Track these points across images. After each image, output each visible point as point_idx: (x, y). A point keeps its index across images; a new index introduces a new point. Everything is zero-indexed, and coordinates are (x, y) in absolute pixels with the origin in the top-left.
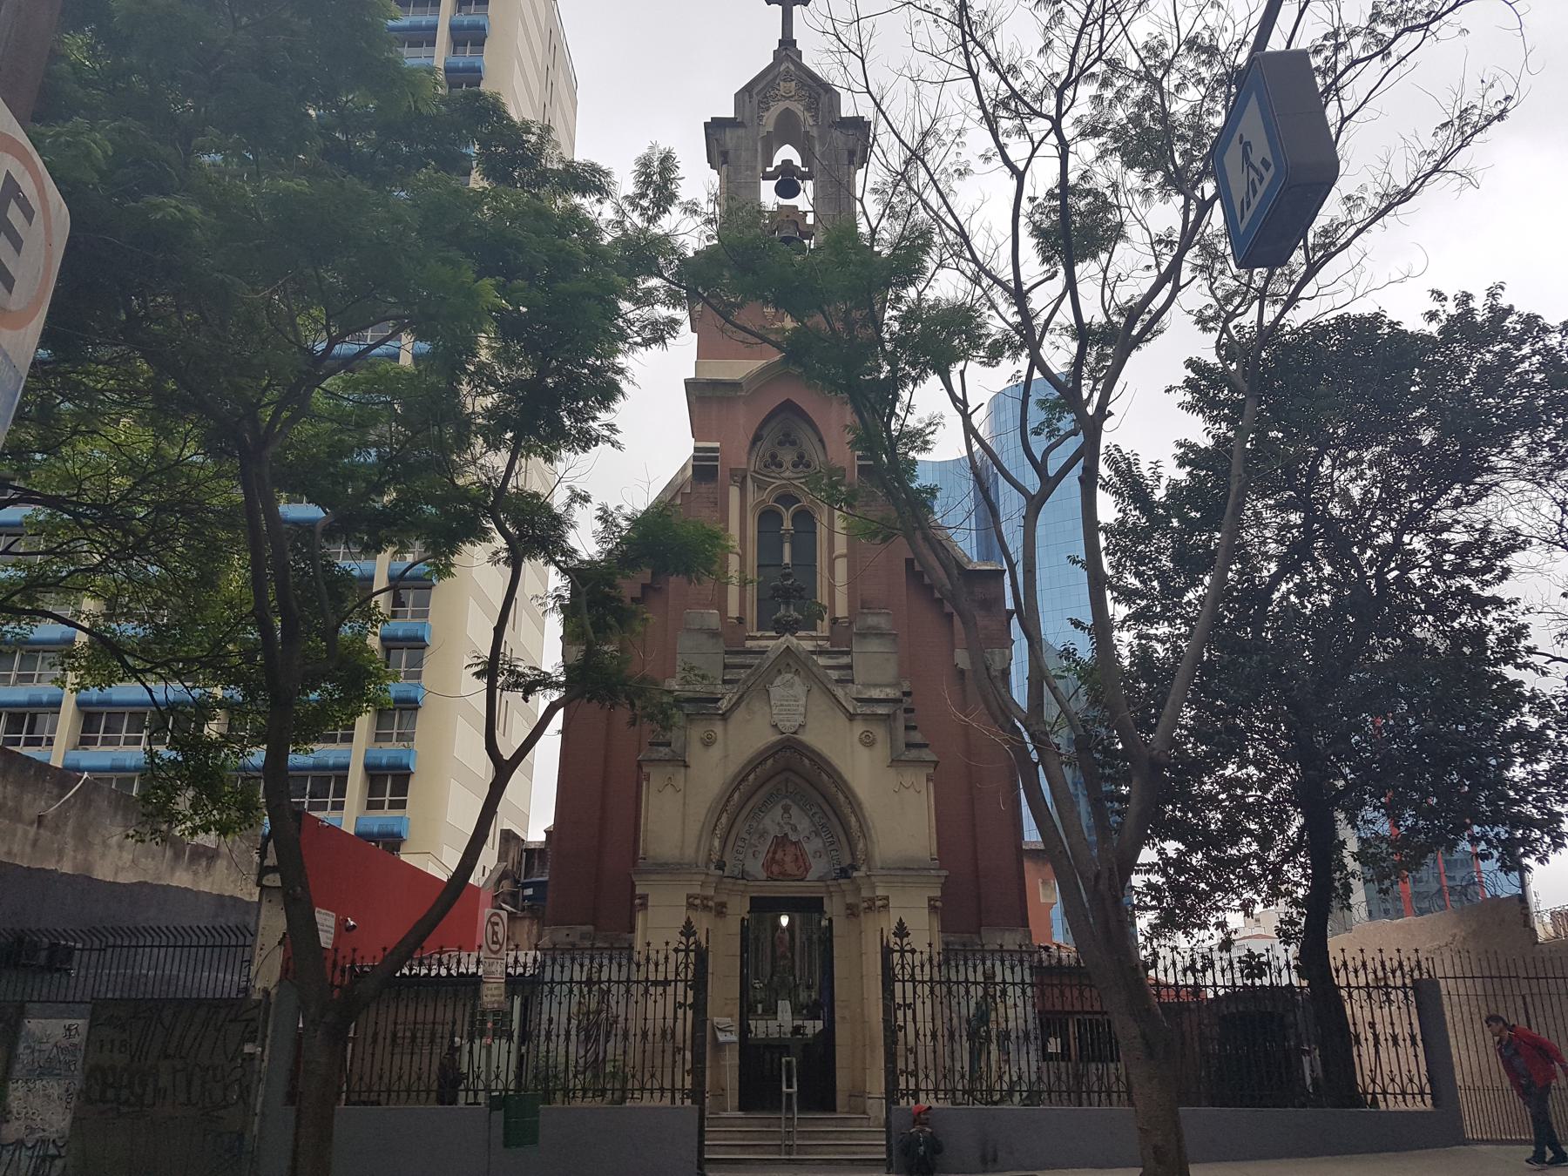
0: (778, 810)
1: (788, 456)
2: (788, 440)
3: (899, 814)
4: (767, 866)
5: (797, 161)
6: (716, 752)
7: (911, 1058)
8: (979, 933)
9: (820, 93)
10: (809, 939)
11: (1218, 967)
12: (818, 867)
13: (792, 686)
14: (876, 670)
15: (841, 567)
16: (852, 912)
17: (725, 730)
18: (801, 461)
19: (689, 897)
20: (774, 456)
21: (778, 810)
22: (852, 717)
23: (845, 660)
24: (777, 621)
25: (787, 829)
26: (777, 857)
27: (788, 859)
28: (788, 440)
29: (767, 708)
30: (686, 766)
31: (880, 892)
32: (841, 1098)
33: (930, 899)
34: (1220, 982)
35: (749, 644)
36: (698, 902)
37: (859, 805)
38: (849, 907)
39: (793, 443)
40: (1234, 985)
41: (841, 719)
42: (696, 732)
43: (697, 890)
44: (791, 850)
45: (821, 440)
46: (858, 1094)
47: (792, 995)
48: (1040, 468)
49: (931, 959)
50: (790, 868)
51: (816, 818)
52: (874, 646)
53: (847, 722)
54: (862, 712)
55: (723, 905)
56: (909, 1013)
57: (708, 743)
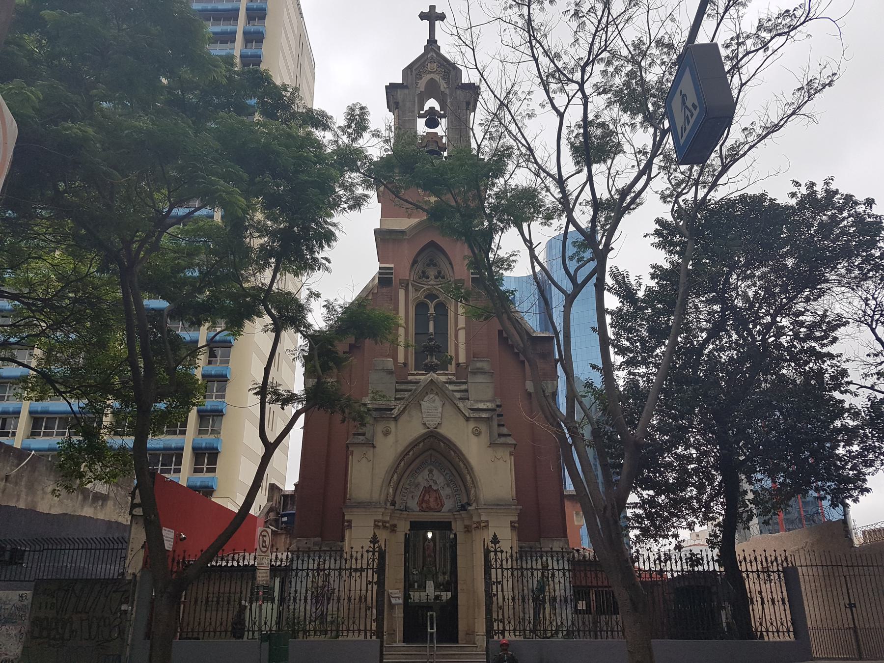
0: (426, 472)
1: (432, 272)
2: (432, 263)
3: (494, 474)
5: (438, 108)
6: (391, 439)
7: (501, 612)
8: (539, 541)
9: (450, 70)
10: (445, 546)
11: (673, 561)
12: (448, 504)
13: (434, 401)
14: (482, 393)
15: (462, 335)
16: (468, 530)
17: (396, 427)
18: (439, 275)
19: (375, 521)
20: (424, 272)
21: (426, 472)
22: (467, 419)
23: (464, 387)
24: (426, 365)
26: (426, 498)
28: (432, 263)
30: (374, 447)
31: (483, 518)
32: (461, 635)
33: (512, 522)
34: (674, 569)
35: (410, 378)
36: (380, 524)
37: (472, 469)
39: (435, 265)
40: (682, 570)
41: (462, 420)
42: (380, 428)
43: (380, 517)
45: (451, 264)
46: (471, 633)
47: (434, 577)
48: (573, 279)
49: (512, 556)
50: (432, 504)
51: (447, 477)
52: (480, 379)
54: (474, 417)
55: (395, 526)
56: (500, 586)
57: (386, 433)
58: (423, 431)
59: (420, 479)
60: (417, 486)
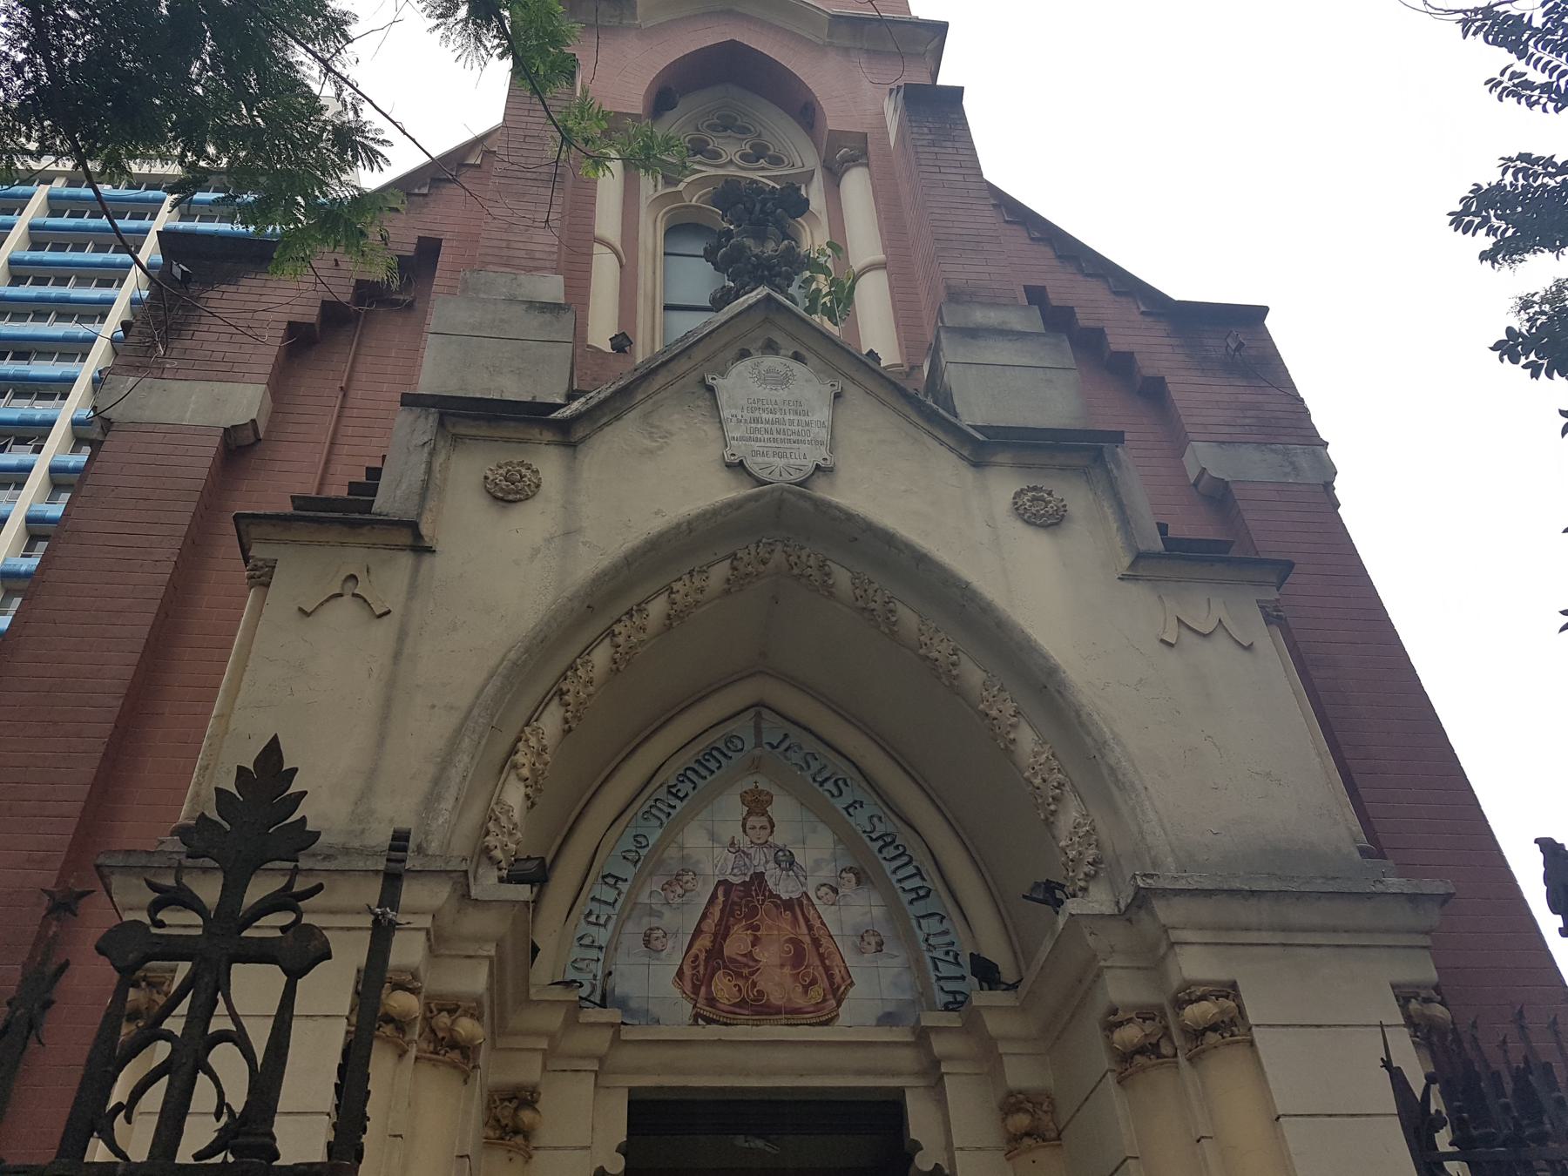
6: (533, 523)
12: (875, 985)
25: (761, 861)
26: (737, 944)
27: (769, 955)
29: (712, 431)
30: (421, 548)
31: (1194, 965)
33: (1404, 994)
38: (1012, 1103)
39: (744, 130)
44: (778, 933)
50: (776, 983)
53: (968, 474)
55: (524, 1097)
57: (508, 493)
58: (722, 491)
59: (695, 839)
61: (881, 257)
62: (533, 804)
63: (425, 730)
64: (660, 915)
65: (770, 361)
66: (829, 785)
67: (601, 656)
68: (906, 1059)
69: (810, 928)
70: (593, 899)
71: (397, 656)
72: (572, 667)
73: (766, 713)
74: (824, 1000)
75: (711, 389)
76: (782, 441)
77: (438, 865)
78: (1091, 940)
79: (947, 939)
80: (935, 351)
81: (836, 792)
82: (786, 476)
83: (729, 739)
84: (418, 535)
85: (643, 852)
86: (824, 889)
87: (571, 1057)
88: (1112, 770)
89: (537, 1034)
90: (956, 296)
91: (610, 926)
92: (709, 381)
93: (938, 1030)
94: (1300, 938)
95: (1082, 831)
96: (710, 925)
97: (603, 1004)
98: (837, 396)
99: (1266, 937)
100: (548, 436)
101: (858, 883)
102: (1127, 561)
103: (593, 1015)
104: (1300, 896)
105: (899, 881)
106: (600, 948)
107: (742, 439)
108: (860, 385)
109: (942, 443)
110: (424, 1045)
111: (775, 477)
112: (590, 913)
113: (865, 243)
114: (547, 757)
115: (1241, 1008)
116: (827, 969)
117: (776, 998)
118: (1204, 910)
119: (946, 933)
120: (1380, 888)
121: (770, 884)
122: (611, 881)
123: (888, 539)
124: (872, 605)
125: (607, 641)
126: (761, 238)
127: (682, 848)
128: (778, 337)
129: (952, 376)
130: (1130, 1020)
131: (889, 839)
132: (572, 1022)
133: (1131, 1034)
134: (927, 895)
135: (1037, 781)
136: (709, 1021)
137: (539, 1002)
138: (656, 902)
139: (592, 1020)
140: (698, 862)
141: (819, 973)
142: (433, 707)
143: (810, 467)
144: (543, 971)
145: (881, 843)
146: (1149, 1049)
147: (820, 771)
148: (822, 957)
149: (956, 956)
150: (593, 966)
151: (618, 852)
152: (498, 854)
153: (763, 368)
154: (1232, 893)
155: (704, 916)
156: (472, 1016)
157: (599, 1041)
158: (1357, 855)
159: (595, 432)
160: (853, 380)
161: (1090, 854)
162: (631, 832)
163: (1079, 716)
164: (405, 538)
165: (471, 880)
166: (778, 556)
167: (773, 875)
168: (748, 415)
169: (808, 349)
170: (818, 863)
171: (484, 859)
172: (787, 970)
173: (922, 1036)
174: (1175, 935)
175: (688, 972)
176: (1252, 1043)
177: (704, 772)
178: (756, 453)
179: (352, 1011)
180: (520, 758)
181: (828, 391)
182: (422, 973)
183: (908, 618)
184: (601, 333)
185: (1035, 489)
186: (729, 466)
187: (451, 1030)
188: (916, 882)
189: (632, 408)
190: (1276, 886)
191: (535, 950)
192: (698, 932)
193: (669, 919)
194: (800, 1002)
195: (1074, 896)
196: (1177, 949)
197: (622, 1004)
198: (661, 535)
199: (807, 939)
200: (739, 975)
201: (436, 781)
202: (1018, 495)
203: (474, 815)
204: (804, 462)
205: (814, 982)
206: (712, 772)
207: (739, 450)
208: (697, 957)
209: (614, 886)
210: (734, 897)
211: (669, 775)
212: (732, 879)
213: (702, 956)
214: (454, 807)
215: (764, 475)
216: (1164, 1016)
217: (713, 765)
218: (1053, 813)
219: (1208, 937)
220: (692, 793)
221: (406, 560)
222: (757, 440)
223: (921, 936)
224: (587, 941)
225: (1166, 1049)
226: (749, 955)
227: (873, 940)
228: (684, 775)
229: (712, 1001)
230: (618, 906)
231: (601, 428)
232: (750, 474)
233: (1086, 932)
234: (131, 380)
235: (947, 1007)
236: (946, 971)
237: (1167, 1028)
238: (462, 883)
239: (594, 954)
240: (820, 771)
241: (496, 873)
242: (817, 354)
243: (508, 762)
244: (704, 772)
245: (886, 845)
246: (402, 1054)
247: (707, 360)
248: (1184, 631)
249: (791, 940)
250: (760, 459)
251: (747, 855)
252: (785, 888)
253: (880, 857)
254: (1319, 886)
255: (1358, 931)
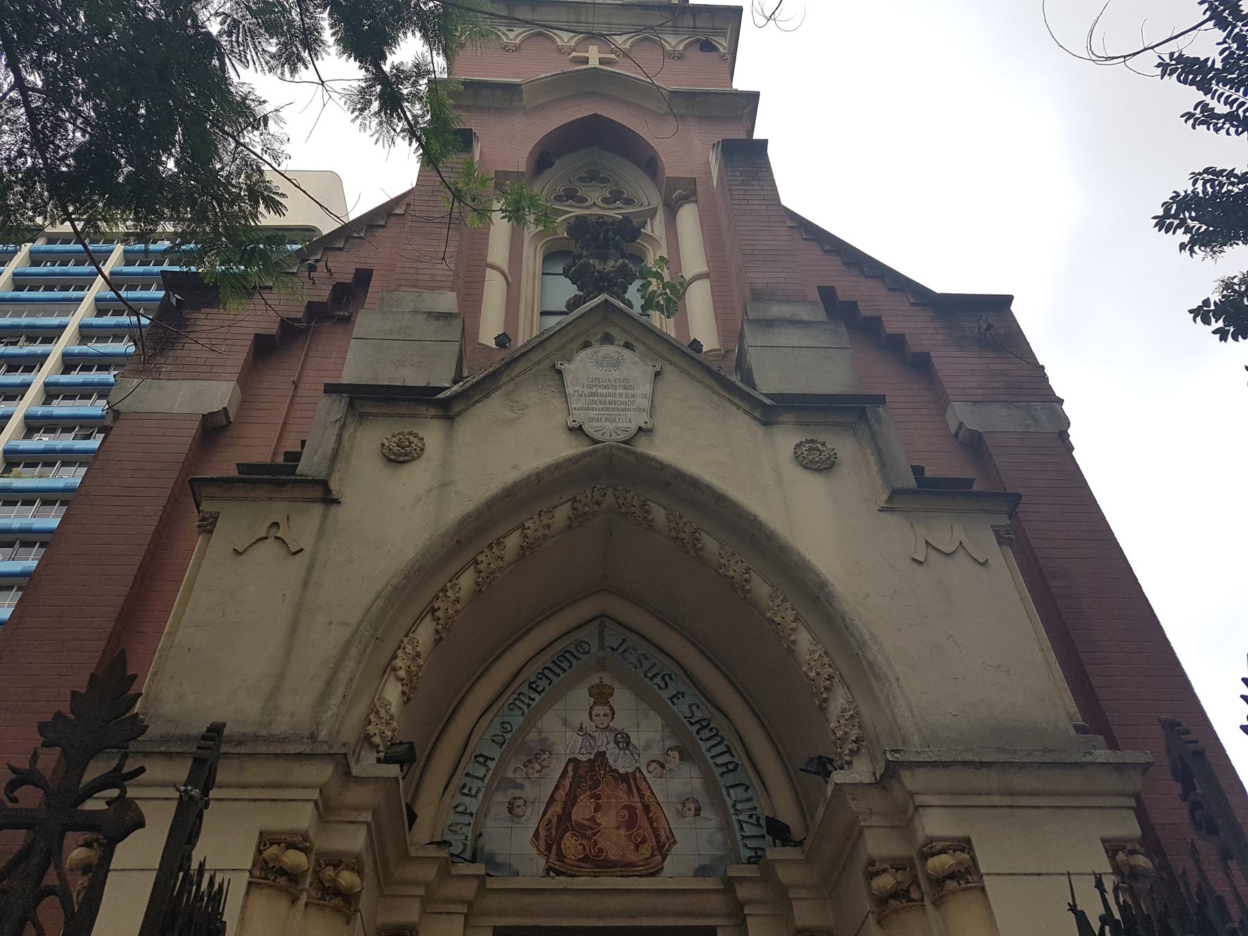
0: (580, 697)
4: (549, 842)
6: (418, 477)
12: (694, 842)
21: (580, 697)
25: (603, 742)
26: (581, 812)
27: (608, 820)
29: (558, 403)
30: (329, 500)
31: (935, 824)
33: (1112, 848)
36: (294, 858)
43: (302, 818)
50: (613, 841)
51: (682, 707)
53: (759, 431)
57: (399, 456)
58: (566, 448)
59: (550, 725)
60: (539, 754)
61: (705, 269)
62: (409, 699)
63: (322, 642)
64: (521, 787)
65: (607, 349)
66: (658, 680)
67: (467, 581)
68: (716, 902)
69: (642, 796)
70: (467, 775)
71: (305, 584)
72: (444, 590)
73: (608, 623)
74: (652, 856)
75: (559, 372)
76: (613, 409)
77: (324, 749)
78: (852, 804)
79: (750, 805)
80: (741, 337)
81: (663, 686)
82: (615, 437)
83: (578, 644)
84: (327, 490)
85: (508, 736)
86: (654, 765)
87: (447, 901)
88: (871, 664)
89: (418, 884)
90: (758, 296)
91: (480, 796)
92: (559, 366)
93: (741, 879)
94: (1025, 801)
95: (847, 715)
96: (561, 794)
97: (473, 860)
98: (657, 374)
99: (996, 800)
100: (432, 411)
101: (682, 758)
102: (885, 496)
103: (464, 868)
104: (1023, 766)
105: (713, 757)
106: (471, 814)
107: (581, 409)
108: (675, 365)
109: (739, 407)
110: (313, 893)
111: (606, 437)
112: (464, 786)
113: (693, 259)
114: (421, 661)
115: (973, 859)
116: (654, 830)
117: (613, 854)
118: (943, 779)
119: (749, 800)
120: (1089, 759)
121: (611, 762)
122: (482, 760)
123: (694, 483)
124: (683, 535)
125: (472, 568)
126: (604, 258)
127: (540, 732)
128: (613, 331)
129: (753, 357)
130: (885, 870)
131: (705, 723)
132: (445, 873)
133: (885, 882)
134: (735, 769)
135: (812, 674)
136: (559, 873)
137: (417, 858)
138: (519, 777)
139: (461, 872)
140: (553, 743)
141: (648, 833)
142: (330, 623)
143: (634, 428)
144: (423, 831)
145: (698, 726)
146: (899, 894)
147: (650, 669)
148: (651, 821)
149: (758, 819)
150: (465, 829)
151: (487, 736)
152: (377, 740)
153: (600, 355)
154: (965, 764)
155: (557, 788)
156: (353, 870)
157: (468, 890)
158: (1073, 732)
159: (468, 408)
160: (670, 362)
161: (854, 734)
162: (498, 720)
163: (844, 620)
164: (318, 493)
165: (352, 762)
166: (610, 498)
167: (612, 753)
168: (587, 391)
169: (637, 339)
170: (648, 746)
171: (367, 745)
172: (622, 832)
173: (729, 884)
174: (920, 800)
175: (542, 833)
176: (983, 889)
177: (558, 671)
178: (593, 419)
179: (254, 865)
180: (398, 662)
181: (651, 371)
182: (311, 835)
183: (710, 544)
184: (489, 332)
185: (812, 441)
186: (571, 429)
187: (334, 880)
188: (726, 759)
189: (499, 388)
190: (1002, 758)
191: (412, 817)
192: (552, 799)
193: (529, 792)
194: (632, 857)
195: (842, 768)
196: (921, 810)
197: (490, 861)
198: (515, 484)
199: (639, 806)
200: (584, 836)
201: (330, 682)
202: (798, 446)
203: (360, 709)
204: (629, 425)
205: (644, 841)
206: (565, 670)
207: (579, 417)
208: (550, 821)
209: (484, 764)
210: (581, 772)
211: (529, 674)
212: (580, 757)
213: (555, 820)
214: (342, 703)
215: (598, 436)
216: (913, 867)
217: (565, 665)
218: (826, 700)
219: (947, 800)
220: (548, 688)
221: (318, 509)
222: (593, 409)
223: (729, 803)
224: (460, 809)
225: (914, 894)
226: (592, 819)
227: (692, 806)
228: (542, 673)
229: (561, 856)
230: (487, 779)
231: (473, 404)
232: (587, 436)
233: (849, 798)
234: (136, 381)
235: (749, 862)
236: (749, 830)
237: (916, 877)
238: (342, 764)
239: (466, 819)
240: (650, 669)
241: (375, 755)
242: (643, 343)
243: (389, 667)
244: (558, 671)
245: (702, 728)
246: (294, 901)
247: (558, 350)
248: (931, 551)
249: (626, 807)
250: (595, 424)
251: (593, 737)
252: (622, 763)
253: (697, 737)
254: (1038, 757)
255: (1074, 794)
